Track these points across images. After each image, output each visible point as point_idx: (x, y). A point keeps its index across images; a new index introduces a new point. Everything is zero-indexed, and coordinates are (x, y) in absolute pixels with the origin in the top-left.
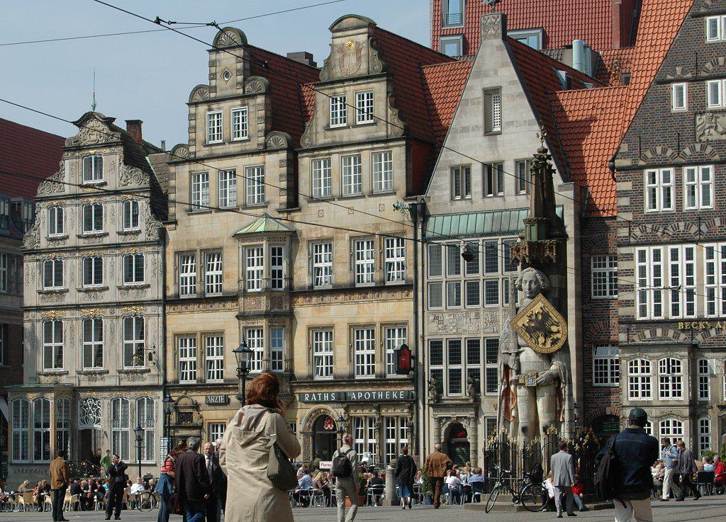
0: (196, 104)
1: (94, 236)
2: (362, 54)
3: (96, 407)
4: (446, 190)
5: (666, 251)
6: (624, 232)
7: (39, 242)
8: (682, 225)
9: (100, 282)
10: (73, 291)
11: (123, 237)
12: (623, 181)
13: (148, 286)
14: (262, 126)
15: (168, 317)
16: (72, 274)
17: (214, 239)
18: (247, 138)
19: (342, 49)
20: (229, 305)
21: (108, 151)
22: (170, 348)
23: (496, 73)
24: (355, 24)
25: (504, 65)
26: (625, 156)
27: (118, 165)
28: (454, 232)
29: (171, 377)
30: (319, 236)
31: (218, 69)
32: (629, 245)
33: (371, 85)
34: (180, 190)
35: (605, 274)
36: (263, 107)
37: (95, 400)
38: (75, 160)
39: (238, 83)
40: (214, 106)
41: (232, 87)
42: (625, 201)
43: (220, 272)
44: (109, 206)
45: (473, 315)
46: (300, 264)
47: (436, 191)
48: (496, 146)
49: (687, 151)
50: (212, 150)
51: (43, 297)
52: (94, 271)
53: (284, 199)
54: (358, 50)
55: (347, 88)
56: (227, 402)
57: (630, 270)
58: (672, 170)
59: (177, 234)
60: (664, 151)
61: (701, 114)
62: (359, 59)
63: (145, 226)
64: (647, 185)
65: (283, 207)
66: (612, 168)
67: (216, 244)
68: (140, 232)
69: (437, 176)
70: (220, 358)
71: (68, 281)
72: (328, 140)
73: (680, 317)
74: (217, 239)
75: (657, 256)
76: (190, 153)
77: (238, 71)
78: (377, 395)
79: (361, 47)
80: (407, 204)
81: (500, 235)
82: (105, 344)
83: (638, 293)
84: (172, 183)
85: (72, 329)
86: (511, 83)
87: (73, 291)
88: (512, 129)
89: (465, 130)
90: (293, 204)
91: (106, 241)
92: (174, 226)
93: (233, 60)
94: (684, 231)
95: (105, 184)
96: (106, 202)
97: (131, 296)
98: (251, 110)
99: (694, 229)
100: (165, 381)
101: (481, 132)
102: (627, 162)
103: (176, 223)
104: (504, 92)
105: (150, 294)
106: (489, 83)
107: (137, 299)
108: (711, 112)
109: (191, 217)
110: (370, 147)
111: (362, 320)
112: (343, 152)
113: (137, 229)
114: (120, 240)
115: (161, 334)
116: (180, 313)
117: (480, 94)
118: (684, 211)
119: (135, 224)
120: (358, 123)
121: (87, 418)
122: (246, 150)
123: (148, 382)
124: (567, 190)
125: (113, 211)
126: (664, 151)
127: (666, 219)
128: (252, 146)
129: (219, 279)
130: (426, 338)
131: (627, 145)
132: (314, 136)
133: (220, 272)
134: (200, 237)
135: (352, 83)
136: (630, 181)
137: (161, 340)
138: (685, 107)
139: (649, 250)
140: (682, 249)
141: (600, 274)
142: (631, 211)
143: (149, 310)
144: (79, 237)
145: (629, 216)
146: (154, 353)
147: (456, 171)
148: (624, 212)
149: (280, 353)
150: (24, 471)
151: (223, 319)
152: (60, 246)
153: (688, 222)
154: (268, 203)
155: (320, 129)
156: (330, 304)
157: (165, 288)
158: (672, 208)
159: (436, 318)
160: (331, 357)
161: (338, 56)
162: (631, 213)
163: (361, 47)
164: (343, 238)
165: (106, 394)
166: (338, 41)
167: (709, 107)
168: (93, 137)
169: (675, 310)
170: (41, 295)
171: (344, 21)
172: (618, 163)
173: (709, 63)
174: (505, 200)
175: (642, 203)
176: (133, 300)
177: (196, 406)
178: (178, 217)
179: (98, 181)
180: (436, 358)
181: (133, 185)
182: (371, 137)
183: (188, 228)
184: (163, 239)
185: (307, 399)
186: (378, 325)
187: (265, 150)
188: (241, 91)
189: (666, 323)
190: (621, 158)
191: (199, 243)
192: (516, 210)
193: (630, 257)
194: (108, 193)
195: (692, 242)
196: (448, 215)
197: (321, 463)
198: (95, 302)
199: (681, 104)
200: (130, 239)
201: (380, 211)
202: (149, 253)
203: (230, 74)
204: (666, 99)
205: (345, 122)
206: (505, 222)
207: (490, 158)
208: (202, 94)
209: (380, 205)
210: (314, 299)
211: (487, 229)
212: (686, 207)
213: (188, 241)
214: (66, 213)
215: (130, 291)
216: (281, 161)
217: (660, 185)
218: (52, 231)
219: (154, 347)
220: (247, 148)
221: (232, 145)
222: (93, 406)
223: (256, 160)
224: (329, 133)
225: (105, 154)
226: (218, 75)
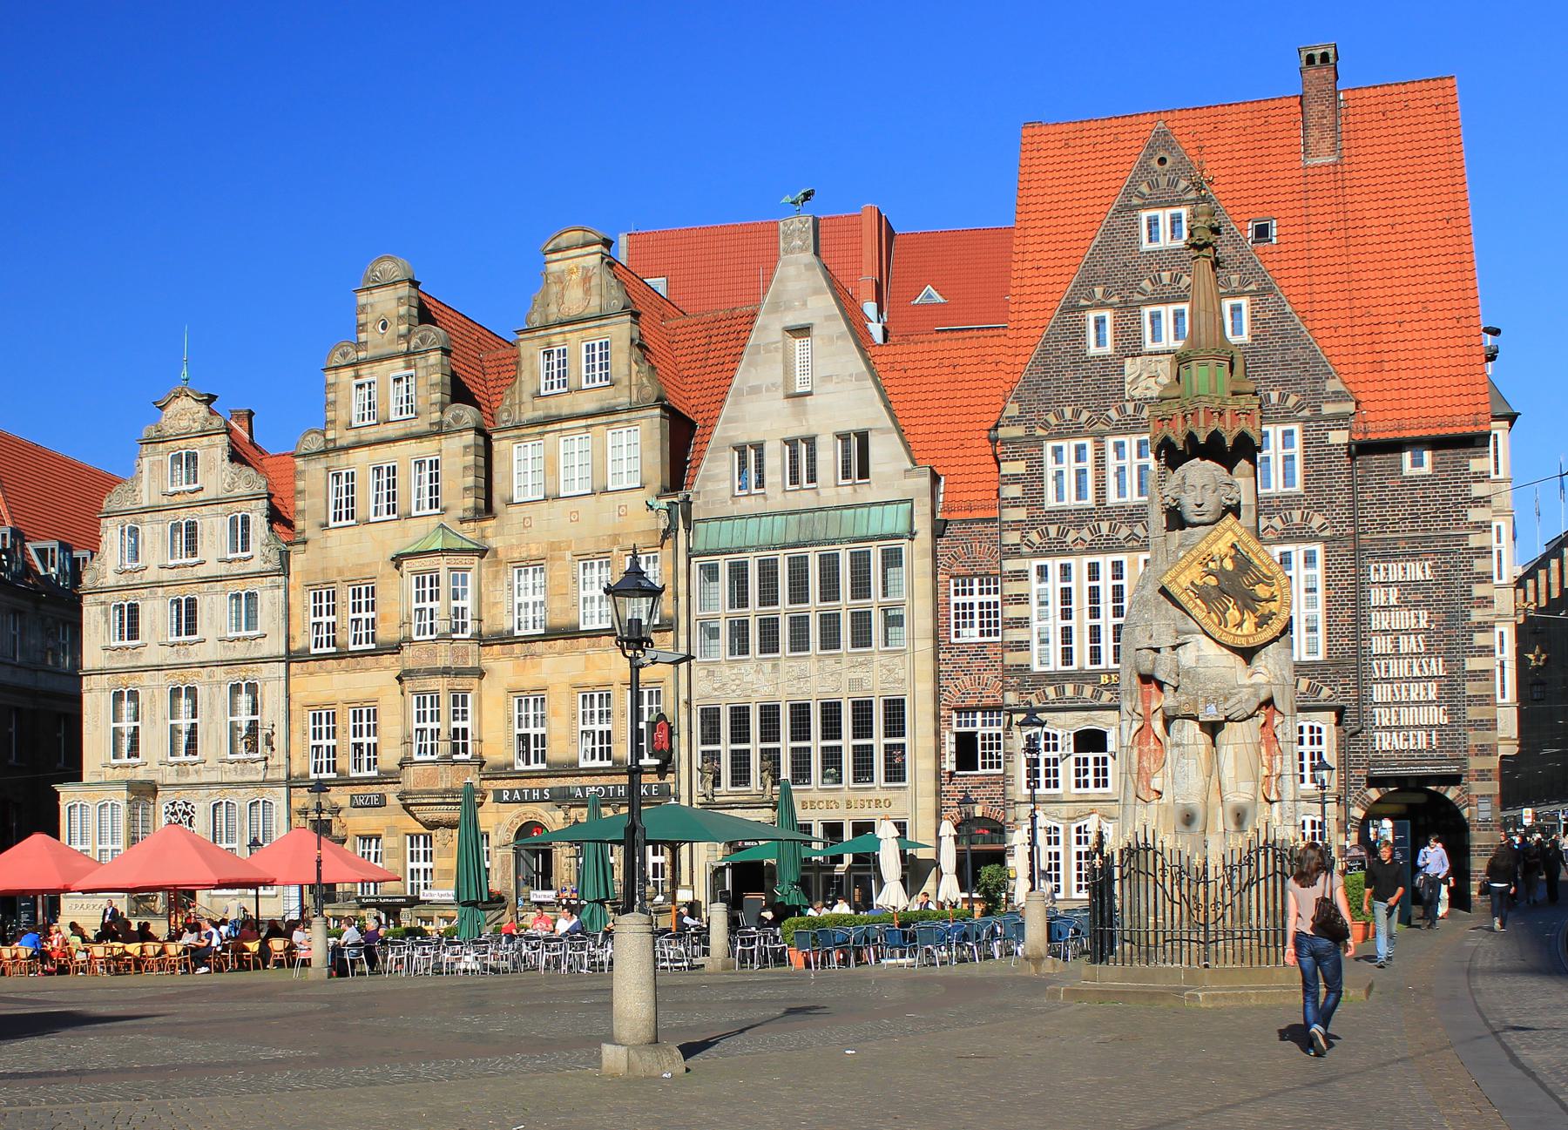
0: (336, 368)
1: (185, 566)
2: (592, 284)
3: (188, 814)
4: (725, 480)
5: (1080, 565)
6: (1012, 538)
8: (1105, 526)
9: (194, 633)
10: (153, 645)
12: (1011, 460)
14: (436, 397)
16: (153, 622)
17: (363, 565)
18: (413, 415)
19: (560, 280)
20: (387, 659)
22: (295, 726)
23: (805, 304)
24: (581, 242)
25: (817, 292)
26: (1013, 421)
27: (219, 462)
28: (738, 543)
29: (296, 771)
30: (524, 555)
31: (371, 317)
32: (1021, 556)
33: (606, 330)
35: (971, 605)
36: (438, 368)
37: (187, 804)
39: (400, 336)
40: (365, 370)
41: (391, 342)
42: (1013, 491)
43: (371, 615)
45: (768, 666)
46: (495, 598)
47: (709, 484)
48: (805, 413)
49: (1113, 413)
50: (360, 435)
51: (110, 656)
52: (188, 616)
53: (470, 502)
54: (586, 279)
55: (568, 336)
56: (382, 802)
57: (1023, 595)
58: (1089, 442)
60: (1076, 414)
61: (1133, 356)
62: (587, 291)
63: (261, 550)
64: (1050, 467)
65: (469, 515)
66: (994, 441)
67: (367, 573)
69: (709, 461)
70: (373, 740)
72: (540, 413)
73: (1102, 666)
74: (368, 565)
75: (1066, 569)
76: (327, 441)
77: (400, 317)
78: (615, 790)
79: (590, 274)
80: (663, 503)
81: (811, 545)
82: (201, 722)
83: (1035, 631)
84: (300, 485)
85: (152, 700)
86: (829, 318)
87: (153, 645)
88: (830, 387)
89: (755, 390)
90: (486, 509)
91: (202, 571)
92: (301, 547)
93: (394, 303)
94: (1108, 535)
95: (202, 489)
97: (240, 651)
98: (421, 373)
99: (1124, 532)
100: (289, 776)
101: (781, 393)
102: (1018, 431)
103: (305, 542)
104: (815, 332)
106: (793, 319)
107: (247, 656)
108: (1151, 354)
109: (328, 532)
110: (604, 419)
111: (593, 678)
112: (561, 430)
113: (246, 554)
114: (223, 569)
115: (283, 705)
117: (775, 333)
118: (1108, 505)
119: (245, 548)
120: (584, 386)
122: (412, 434)
124: (919, 475)
125: (214, 530)
126: (1076, 414)
127: (1080, 518)
128: (421, 425)
129: (372, 623)
130: (694, 704)
131: (1017, 405)
132: (517, 407)
133: (371, 615)
135: (575, 327)
136: (1023, 459)
137: (282, 715)
138: (1108, 349)
139: (1053, 565)
140: (1105, 562)
141: (964, 605)
142: (1024, 506)
145: (1021, 514)
146: (273, 733)
147: (741, 450)
148: (1012, 507)
149: (465, 731)
150: (85, 907)
151: (376, 681)
152: (134, 582)
153: (1114, 522)
154: (444, 510)
155: (526, 397)
156: (540, 656)
158: (1090, 501)
159: (711, 673)
160: (543, 736)
161: (555, 289)
162: (1025, 509)
163: (590, 274)
164: (562, 558)
165: (203, 793)
166: (553, 267)
167: (1147, 346)
168: (184, 423)
169: (1095, 656)
170: (108, 653)
171: (565, 236)
172: (1003, 432)
173: (1147, 281)
174: (818, 494)
175: (1041, 493)
176: (242, 656)
177: (337, 810)
178: (307, 535)
179: (193, 487)
180: (711, 735)
181: (241, 490)
182: (606, 406)
183: (324, 551)
184: (284, 569)
185: (505, 797)
186: (617, 686)
187: (439, 431)
188: (404, 347)
189: (1081, 677)
190: (1008, 425)
191: (340, 572)
192: (837, 508)
193: (1021, 576)
194: (205, 503)
195: (1120, 549)
196: (728, 518)
197: (532, 892)
198: (187, 661)
199: (1100, 342)
200: (236, 568)
201: (620, 515)
203: (389, 324)
204: (1079, 334)
205: (564, 386)
206: (818, 527)
207: (795, 431)
208: (344, 355)
209: (620, 507)
210: (518, 648)
211: (791, 539)
212: (1112, 498)
213: (323, 569)
214: (143, 534)
215: (236, 642)
216: (466, 447)
217: (1069, 466)
219: (273, 725)
220: (414, 430)
221: (389, 426)
222: (185, 813)
223: (427, 448)
224: (537, 401)
225: (202, 448)
226: (370, 327)
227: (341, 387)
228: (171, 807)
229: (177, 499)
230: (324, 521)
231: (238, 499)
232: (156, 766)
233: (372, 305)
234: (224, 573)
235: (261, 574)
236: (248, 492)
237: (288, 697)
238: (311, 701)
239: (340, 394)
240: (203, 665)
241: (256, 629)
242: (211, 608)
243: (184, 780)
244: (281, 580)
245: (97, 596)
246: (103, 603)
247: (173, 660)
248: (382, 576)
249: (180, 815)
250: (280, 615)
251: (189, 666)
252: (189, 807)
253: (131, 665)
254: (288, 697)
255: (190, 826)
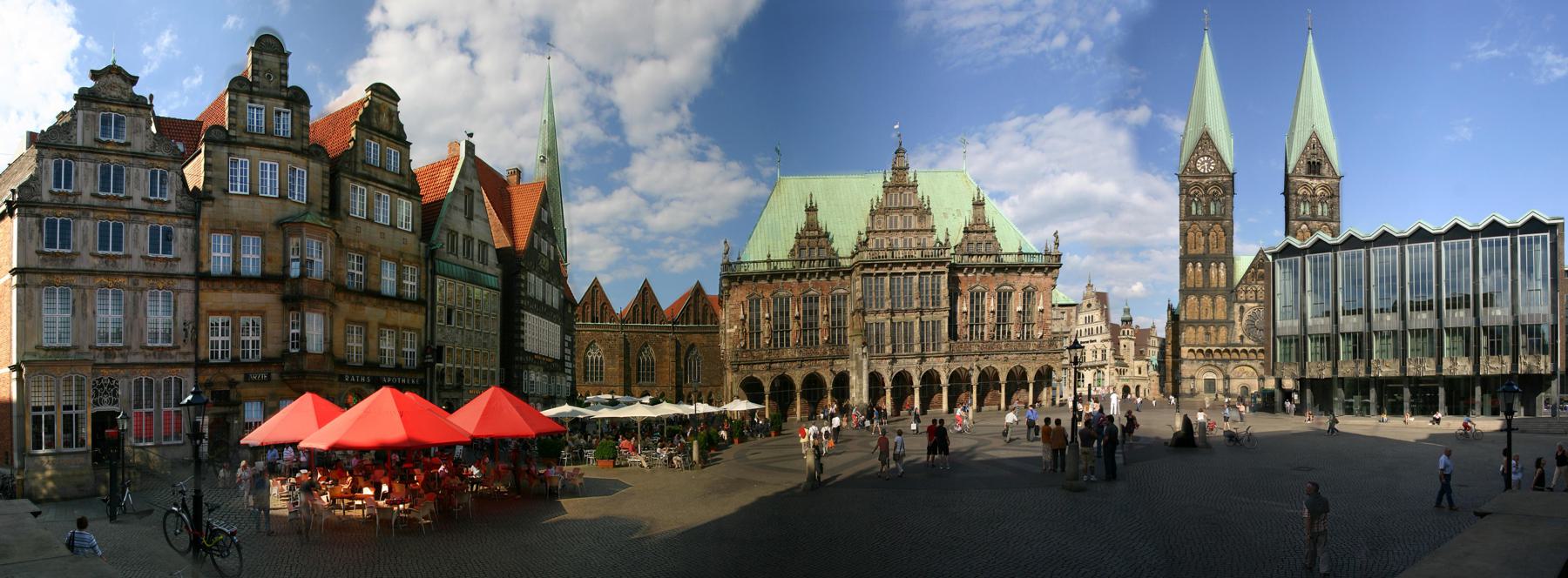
7: (41, 195)
10: (85, 254)
11: (149, 205)
13: (177, 259)
15: (201, 294)
16: (85, 237)
20: (273, 287)
21: (133, 111)
27: (144, 129)
29: (202, 356)
34: (217, 169)
37: (111, 380)
38: (91, 112)
44: (133, 170)
59: (213, 212)
68: (169, 202)
71: (79, 243)
74: (260, 223)
91: (127, 204)
92: (210, 203)
95: (128, 144)
96: (131, 165)
97: (159, 268)
105: (181, 268)
114: (145, 206)
116: (216, 290)
121: (100, 399)
123: (179, 359)
134: (240, 219)
143: (178, 284)
144: (94, 195)
157: (198, 264)
168: (114, 94)
170: (41, 257)
177: (233, 384)
178: (214, 194)
184: (196, 216)
191: (239, 225)
200: (156, 207)
202: (181, 226)
208: (241, 85)
213: (226, 220)
218: (58, 185)
225: (130, 115)
227: (240, 104)
228: (97, 382)
229: (109, 147)
230: (226, 188)
231: (159, 158)
232: (87, 350)
233: (262, 61)
234: (146, 208)
235: (177, 215)
236: (166, 154)
237: (197, 304)
238: (214, 308)
239: (240, 109)
240: (129, 274)
241: (171, 254)
242: (137, 234)
243: (110, 361)
244: (190, 222)
245: (32, 209)
246: (38, 216)
247: (103, 267)
248: (269, 232)
249: (106, 388)
250: (189, 247)
251: (120, 274)
252: (114, 382)
253: (64, 268)
254: (197, 304)
255: (114, 396)
